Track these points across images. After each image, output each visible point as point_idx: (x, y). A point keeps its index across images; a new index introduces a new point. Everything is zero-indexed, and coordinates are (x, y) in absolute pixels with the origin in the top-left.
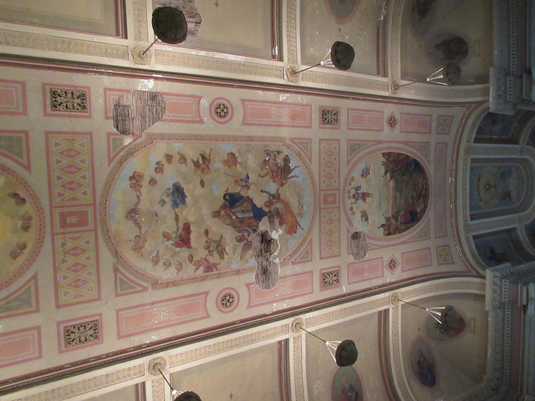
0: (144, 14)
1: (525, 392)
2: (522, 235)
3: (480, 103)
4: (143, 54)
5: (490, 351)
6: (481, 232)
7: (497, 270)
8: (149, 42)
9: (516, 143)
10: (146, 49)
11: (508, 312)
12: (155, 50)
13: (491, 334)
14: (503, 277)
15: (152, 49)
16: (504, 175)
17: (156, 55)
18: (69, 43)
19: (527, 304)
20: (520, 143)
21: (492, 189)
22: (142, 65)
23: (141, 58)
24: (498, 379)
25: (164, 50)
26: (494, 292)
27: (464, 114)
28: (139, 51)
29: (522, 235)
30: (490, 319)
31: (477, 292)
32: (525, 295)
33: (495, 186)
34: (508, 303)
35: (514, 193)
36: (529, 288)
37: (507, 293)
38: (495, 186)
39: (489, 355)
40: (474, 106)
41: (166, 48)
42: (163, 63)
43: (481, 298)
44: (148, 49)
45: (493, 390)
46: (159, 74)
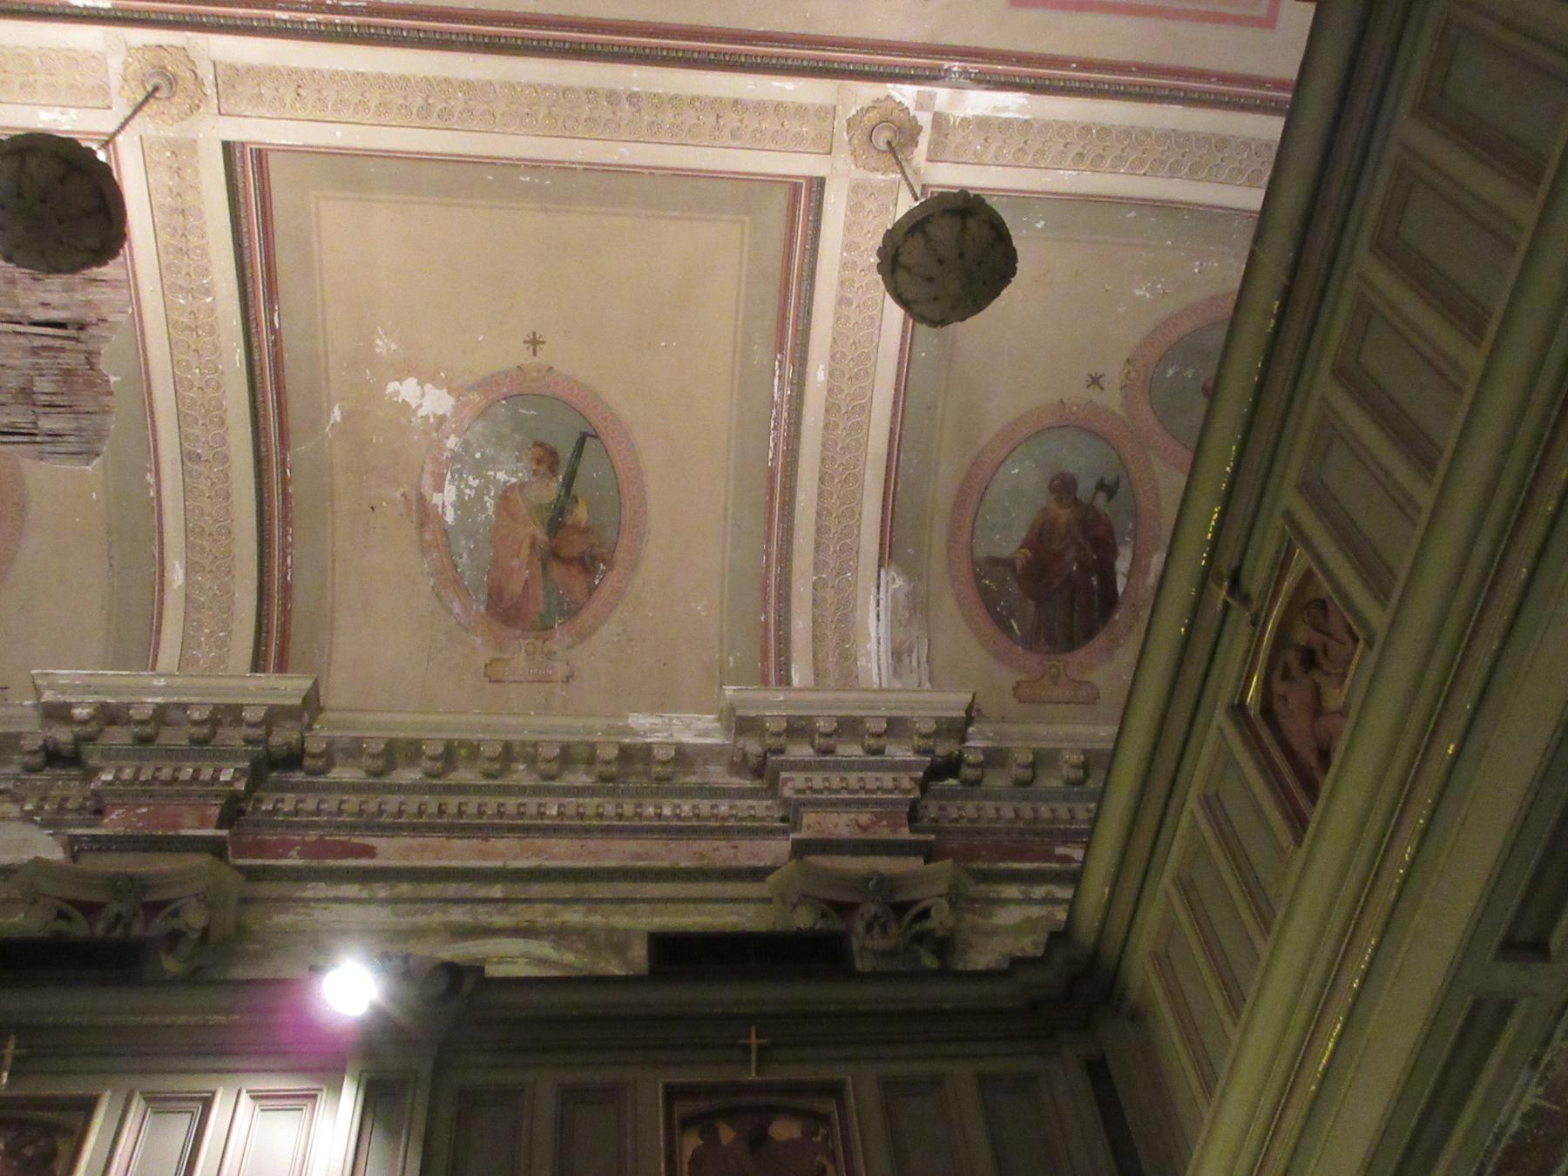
0: (164, 237)
4: (156, 89)
8: (136, 138)
10: (146, 109)
12: (109, 108)
15: (121, 110)
17: (104, 90)
18: (384, 107)
22: (160, 46)
23: (162, 72)
25: (72, 112)
28: (176, 99)
41: (63, 119)
42: (73, 59)
44: (135, 112)
46: (85, 13)
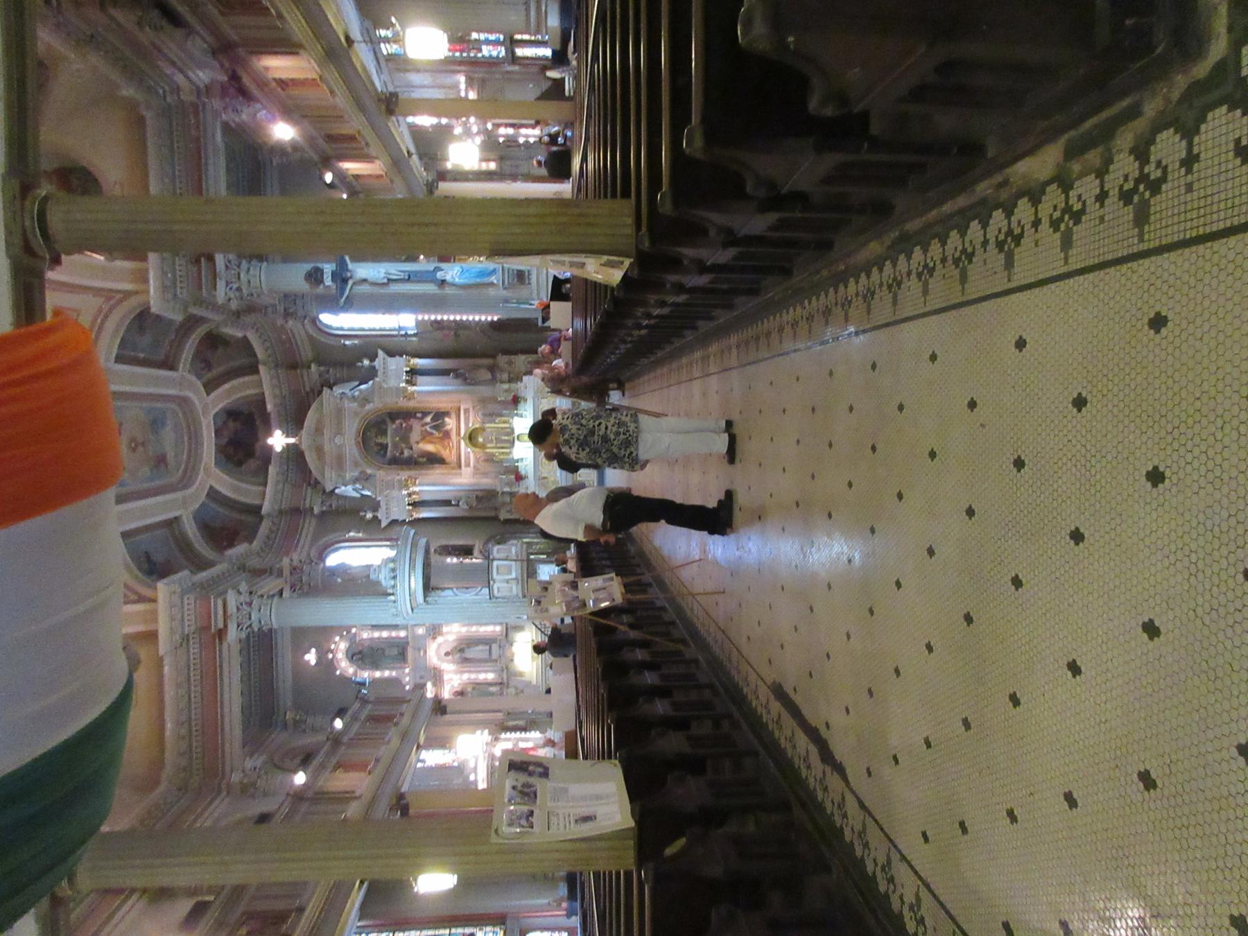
1: (228, 769)
2: (191, 529)
3: (127, 295)
5: (169, 726)
6: (133, 526)
7: (174, 582)
9: (172, 368)
11: (194, 649)
13: (169, 693)
14: (184, 593)
16: (156, 424)
19: (226, 626)
20: (181, 369)
21: (141, 449)
24: (184, 769)
26: (172, 619)
27: (100, 310)
29: (191, 529)
30: (166, 669)
31: (141, 628)
32: (221, 612)
33: (143, 444)
34: (194, 633)
35: (170, 457)
36: (228, 599)
37: (193, 617)
38: (143, 444)
39: (168, 733)
40: (119, 296)
43: (152, 636)
45: (180, 789)
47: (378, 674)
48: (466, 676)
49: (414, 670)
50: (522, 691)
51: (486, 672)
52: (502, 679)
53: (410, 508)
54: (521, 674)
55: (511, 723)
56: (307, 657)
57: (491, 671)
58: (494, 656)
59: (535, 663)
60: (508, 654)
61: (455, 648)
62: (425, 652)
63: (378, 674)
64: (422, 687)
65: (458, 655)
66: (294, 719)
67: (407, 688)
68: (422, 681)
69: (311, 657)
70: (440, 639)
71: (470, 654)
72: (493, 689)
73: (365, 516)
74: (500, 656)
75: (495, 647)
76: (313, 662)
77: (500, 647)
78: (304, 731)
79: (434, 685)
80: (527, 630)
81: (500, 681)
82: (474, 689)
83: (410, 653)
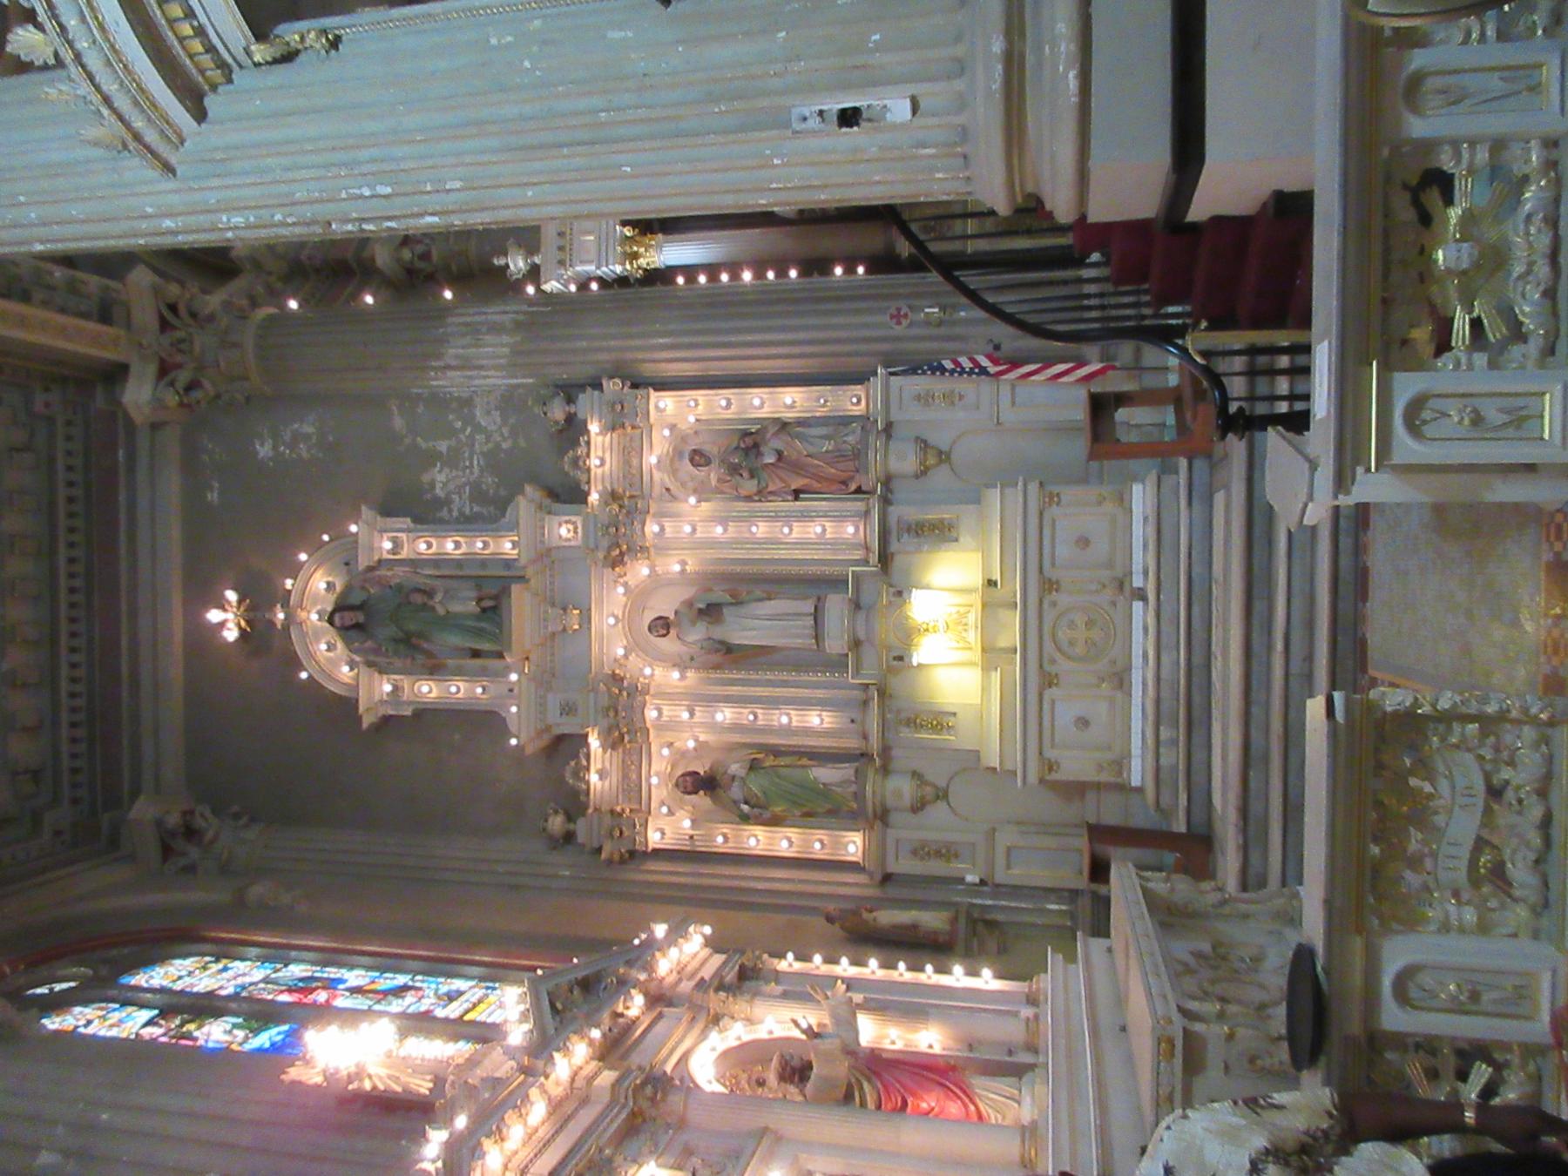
47: (428, 690)
48: (725, 715)
49: (545, 680)
50: (942, 795)
51: (804, 704)
52: (865, 737)
53: (628, 232)
54: (939, 720)
55: (888, 917)
56: (214, 616)
57: (822, 704)
58: (835, 644)
59: (996, 677)
60: (883, 630)
61: (689, 604)
62: (586, 618)
63: (428, 690)
64: (566, 747)
65: (697, 633)
66: (159, 823)
67: (514, 742)
68: (567, 726)
69: (226, 620)
70: (640, 570)
71: (745, 629)
72: (825, 774)
73: (507, 266)
74: (856, 644)
75: (836, 607)
76: (231, 634)
77: (857, 605)
78: (191, 869)
79: (613, 742)
80: (965, 539)
81: (852, 743)
82: (754, 766)
83: (522, 607)
